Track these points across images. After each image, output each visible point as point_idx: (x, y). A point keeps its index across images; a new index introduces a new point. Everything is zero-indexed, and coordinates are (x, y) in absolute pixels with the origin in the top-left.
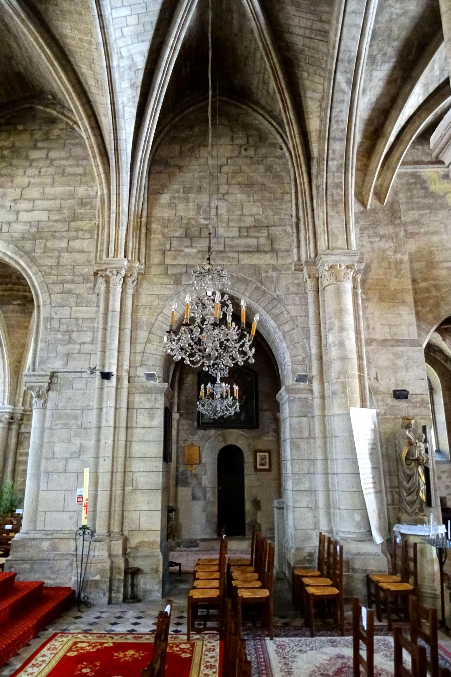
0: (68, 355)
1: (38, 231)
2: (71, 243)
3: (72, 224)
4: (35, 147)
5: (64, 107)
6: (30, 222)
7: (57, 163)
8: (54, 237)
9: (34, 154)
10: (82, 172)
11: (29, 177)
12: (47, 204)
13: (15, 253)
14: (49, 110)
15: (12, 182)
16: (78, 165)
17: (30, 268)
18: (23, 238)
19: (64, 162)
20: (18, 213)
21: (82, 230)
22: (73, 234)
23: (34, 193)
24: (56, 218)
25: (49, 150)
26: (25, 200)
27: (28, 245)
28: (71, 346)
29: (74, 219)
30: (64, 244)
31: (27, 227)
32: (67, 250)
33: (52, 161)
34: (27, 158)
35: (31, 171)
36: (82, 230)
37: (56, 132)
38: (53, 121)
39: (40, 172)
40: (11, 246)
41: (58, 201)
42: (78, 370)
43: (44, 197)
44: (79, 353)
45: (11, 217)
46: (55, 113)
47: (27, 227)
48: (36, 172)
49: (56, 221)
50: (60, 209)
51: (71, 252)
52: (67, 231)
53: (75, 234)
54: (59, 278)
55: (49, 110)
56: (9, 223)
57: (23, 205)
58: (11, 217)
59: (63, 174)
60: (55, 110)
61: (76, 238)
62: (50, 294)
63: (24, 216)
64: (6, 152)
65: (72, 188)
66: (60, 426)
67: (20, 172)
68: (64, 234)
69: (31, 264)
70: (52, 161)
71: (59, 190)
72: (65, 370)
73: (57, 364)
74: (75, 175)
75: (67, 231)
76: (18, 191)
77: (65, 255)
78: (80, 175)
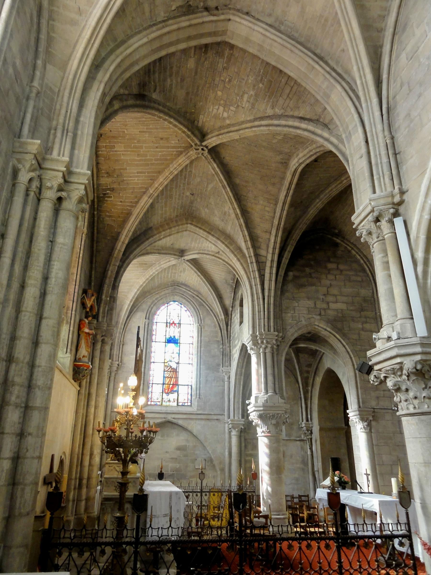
0: (378, 398)
1: (343, 316)
2: (365, 325)
3: (362, 313)
4: (330, 262)
5: (344, 238)
6: (337, 310)
7: (344, 272)
8: (353, 321)
9: (330, 266)
10: (360, 280)
11: (330, 280)
12: (345, 299)
13: (333, 330)
14: (335, 239)
15: (320, 282)
16: (357, 275)
17: (344, 340)
18: (335, 320)
19: (348, 273)
20: (328, 303)
21: (369, 318)
22: (364, 320)
23: (334, 291)
24: (351, 308)
25: (338, 264)
26: (330, 295)
27: (339, 325)
28: (377, 392)
29: (362, 310)
30: (360, 326)
31: (336, 313)
32: (363, 329)
33: (341, 271)
34: (326, 268)
35: (330, 277)
36: (369, 318)
37: (339, 253)
38: (336, 245)
39: (335, 277)
40: (329, 325)
41: (350, 298)
42: (386, 408)
43: (342, 295)
44: (384, 397)
45: (325, 306)
46: (338, 241)
47: (336, 313)
48: (333, 277)
49: (351, 310)
50: (353, 303)
51: (366, 331)
52: (360, 317)
53: (364, 320)
54: (363, 348)
55: (335, 239)
56: (325, 309)
57: (330, 298)
58: (325, 306)
59: (350, 281)
60: (337, 238)
61: (366, 322)
62: (359, 358)
63: (333, 306)
64: (312, 263)
65: (356, 290)
66: (382, 444)
67: (324, 276)
68: (359, 319)
69: (344, 338)
70: (341, 271)
71: (348, 290)
72: (378, 407)
73: (373, 403)
74: (357, 281)
75: (360, 317)
76: (325, 289)
77: (362, 333)
78: (359, 281)
